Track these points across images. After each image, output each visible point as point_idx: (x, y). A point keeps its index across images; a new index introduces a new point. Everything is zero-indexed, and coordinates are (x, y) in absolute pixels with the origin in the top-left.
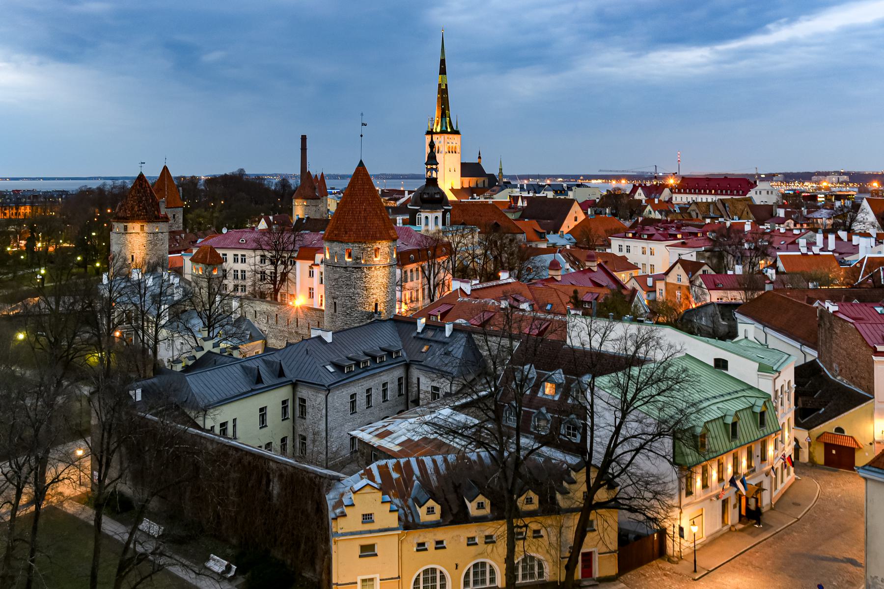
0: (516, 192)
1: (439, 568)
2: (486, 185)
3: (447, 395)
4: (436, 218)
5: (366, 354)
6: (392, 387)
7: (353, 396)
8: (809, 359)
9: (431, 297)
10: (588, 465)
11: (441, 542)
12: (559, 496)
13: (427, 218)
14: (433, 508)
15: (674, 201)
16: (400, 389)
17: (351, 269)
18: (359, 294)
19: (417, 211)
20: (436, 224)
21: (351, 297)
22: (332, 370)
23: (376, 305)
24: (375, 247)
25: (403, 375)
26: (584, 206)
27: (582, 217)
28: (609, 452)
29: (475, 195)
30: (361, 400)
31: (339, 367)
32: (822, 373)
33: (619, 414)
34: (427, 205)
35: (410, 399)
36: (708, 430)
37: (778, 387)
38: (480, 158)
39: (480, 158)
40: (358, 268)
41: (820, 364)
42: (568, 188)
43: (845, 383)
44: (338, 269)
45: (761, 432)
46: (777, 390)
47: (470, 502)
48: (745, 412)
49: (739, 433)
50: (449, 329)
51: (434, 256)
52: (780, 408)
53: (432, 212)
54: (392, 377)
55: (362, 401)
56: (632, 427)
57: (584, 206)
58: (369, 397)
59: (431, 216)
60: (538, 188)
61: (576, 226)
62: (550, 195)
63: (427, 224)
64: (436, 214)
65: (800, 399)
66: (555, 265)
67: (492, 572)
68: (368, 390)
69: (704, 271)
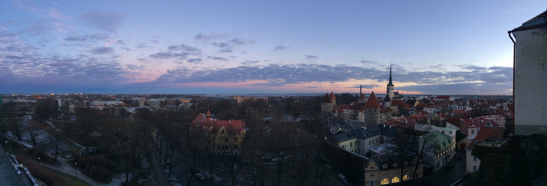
3: (390, 141)
4: (389, 103)
6: (378, 139)
7: (370, 141)
9: (387, 120)
10: (417, 155)
12: (412, 162)
16: (380, 140)
19: (385, 102)
20: (389, 105)
28: (422, 152)
30: (372, 142)
31: (367, 135)
33: (424, 144)
51: (388, 112)
54: (378, 137)
56: (426, 146)
59: (388, 103)
63: (387, 105)
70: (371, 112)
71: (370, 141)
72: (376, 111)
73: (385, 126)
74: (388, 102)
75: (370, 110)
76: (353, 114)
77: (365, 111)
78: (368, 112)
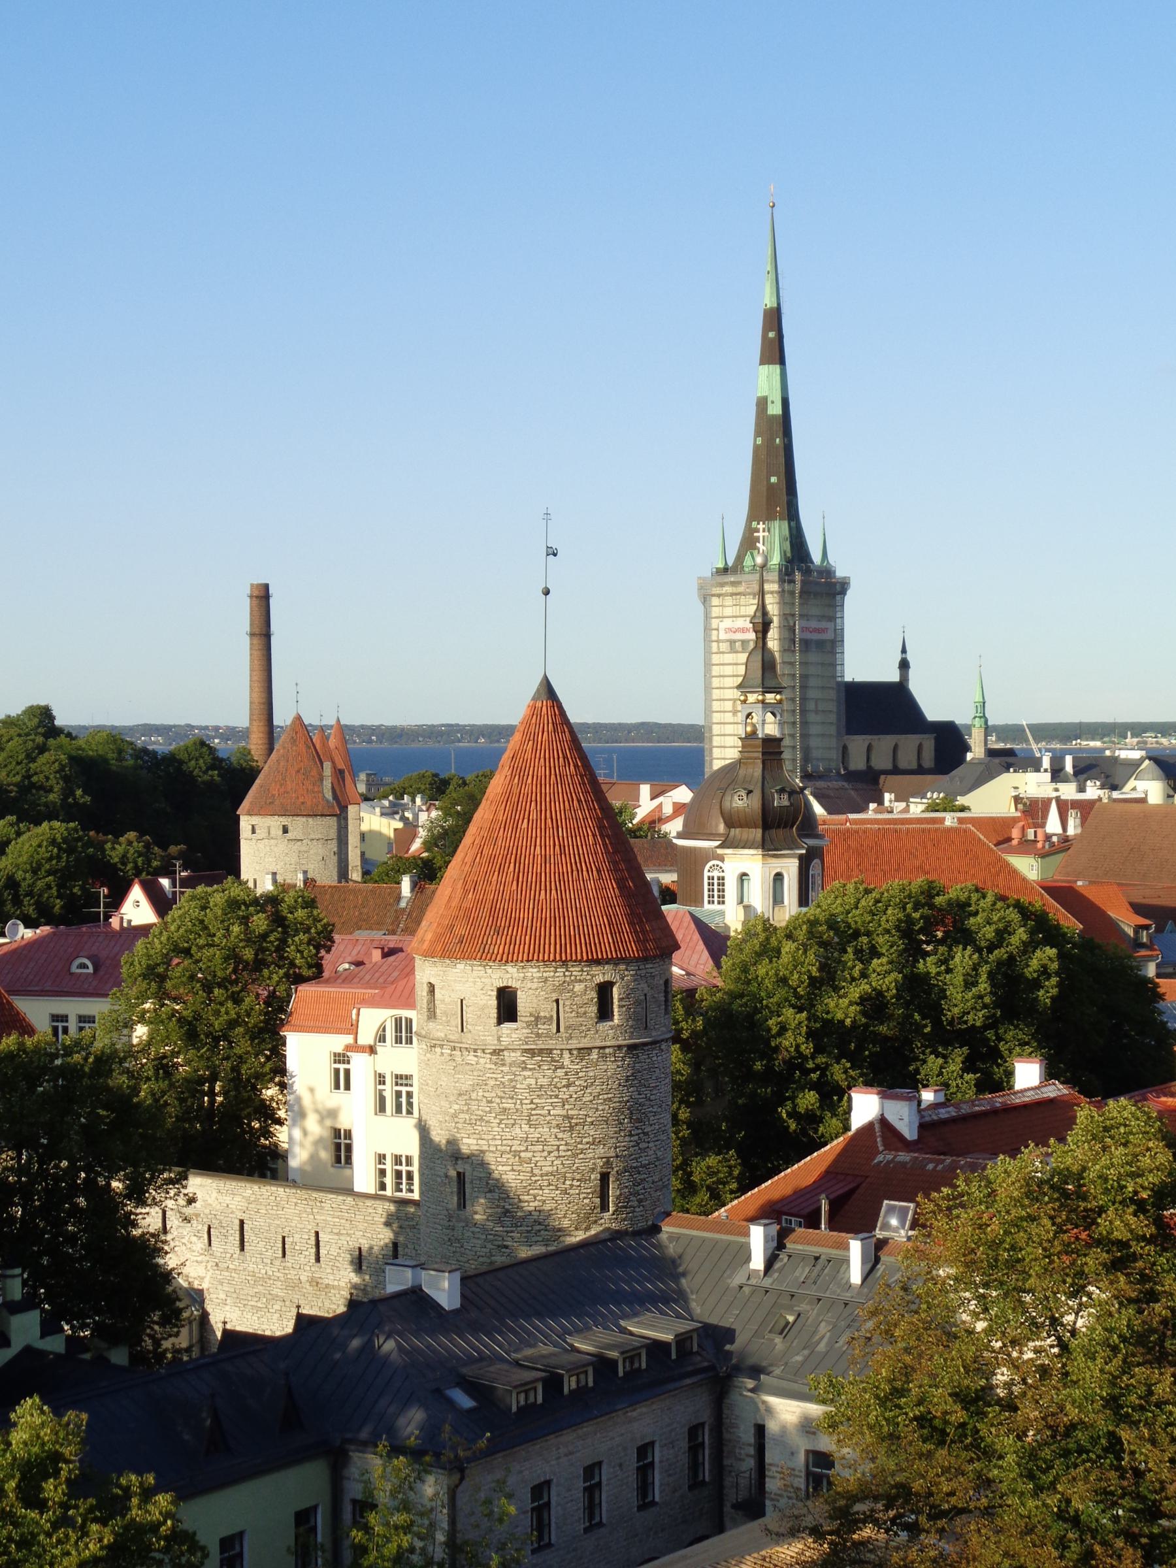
0: (1035, 784)
2: (928, 760)
4: (779, 877)
13: (743, 877)
16: (695, 1466)
17: (516, 1056)
18: (545, 1143)
21: (516, 1154)
22: (465, 1401)
23: (604, 1178)
24: (600, 979)
25: (706, 1416)
34: (736, 832)
35: (731, 1497)
38: (904, 665)
39: (904, 665)
44: (471, 1058)
64: (777, 865)
68: (591, 1470)
70: (537, 1018)
74: (769, 847)
77: (432, 1014)
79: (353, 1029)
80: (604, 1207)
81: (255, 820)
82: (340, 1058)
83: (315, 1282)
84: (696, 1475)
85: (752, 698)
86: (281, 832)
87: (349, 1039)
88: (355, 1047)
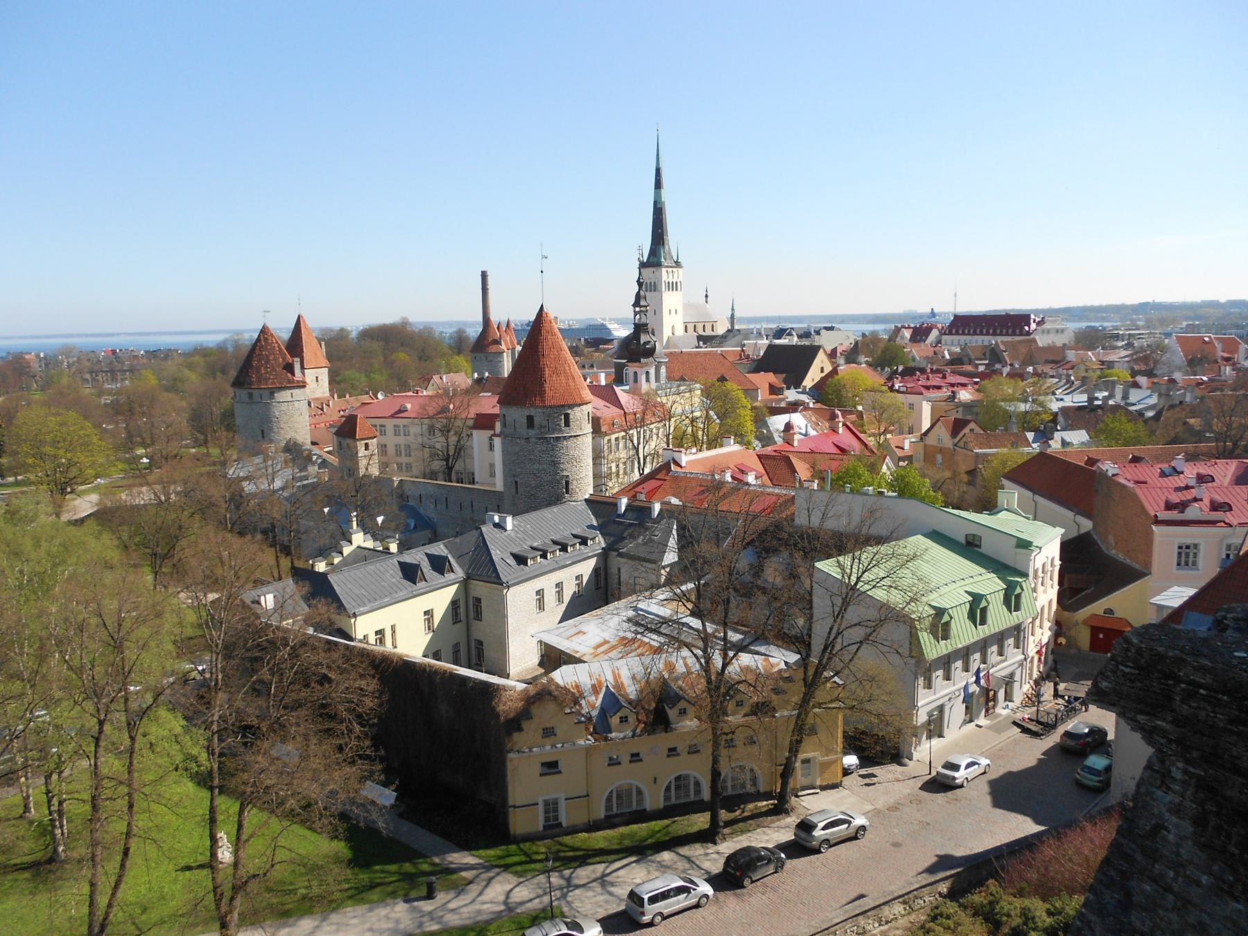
1: (633, 782)
5: (555, 543)
7: (540, 593)
8: (1083, 531)
11: (637, 755)
14: (626, 717)
15: (943, 342)
16: (597, 582)
19: (624, 365)
20: (648, 380)
21: (535, 474)
22: (512, 561)
26: (832, 355)
27: (828, 368)
29: (701, 343)
30: (550, 596)
31: (521, 560)
32: (1096, 547)
33: (839, 601)
36: (951, 618)
37: (1039, 565)
38: (706, 296)
39: (706, 296)
40: (542, 438)
41: (1095, 537)
42: (815, 331)
43: (1121, 557)
44: (518, 441)
45: (1015, 617)
46: (1038, 569)
47: (670, 708)
48: (996, 594)
49: (989, 620)
50: (657, 507)
52: (1040, 589)
53: (641, 367)
54: (586, 568)
55: (550, 598)
57: (832, 355)
58: (560, 594)
60: (780, 333)
61: (822, 378)
62: (795, 340)
63: (636, 381)
64: (646, 369)
65: (1066, 580)
66: (788, 427)
67: (697, 784)
68: (559, 585)
69: (972, 430)
70: (541, 426)
71: (538, 593)
72: (567, 424)
73: (624, 501)
75: (530, 420)
76: (438, 446)
78: (523, 430)
79: (492, 427)
80: (567, 493)
81: (476, 355)
82: (491, 439)
83: (472, 519)
84: (598, 584)
85: (637, 309)
86: (483, 358)
87: (492, 432)
88: (494, 435)
